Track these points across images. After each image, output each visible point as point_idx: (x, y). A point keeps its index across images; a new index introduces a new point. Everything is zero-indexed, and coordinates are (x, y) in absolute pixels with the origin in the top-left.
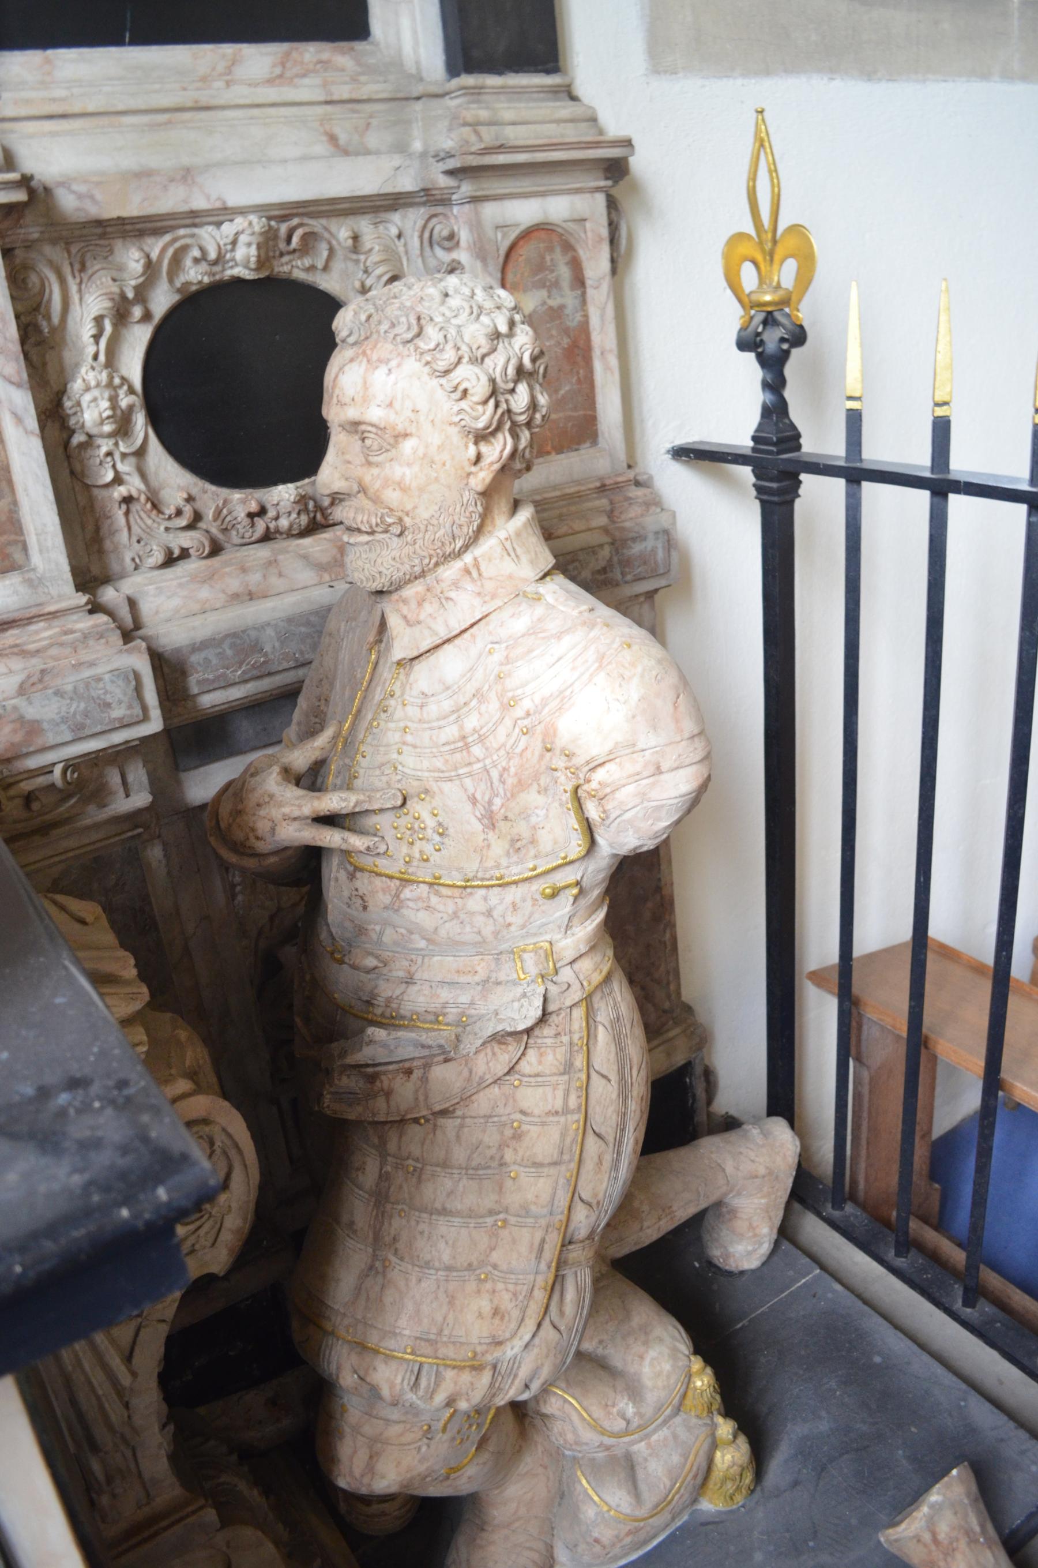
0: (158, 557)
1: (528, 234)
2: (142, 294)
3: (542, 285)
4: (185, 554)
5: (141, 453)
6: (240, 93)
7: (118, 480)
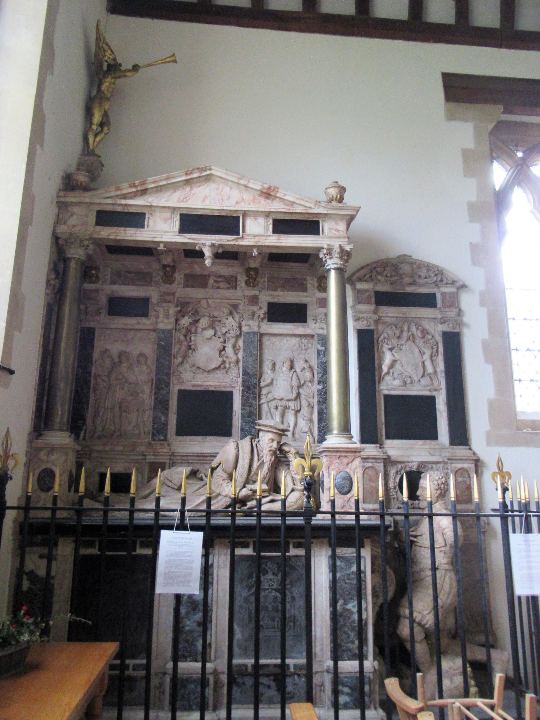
0: (397, 507)
1: (460, 469)
2: (400, 470)
3: (462, 477)
4: (401, 508)
5: (397, 492)
6: (418, 446)
7: (393, 495)
